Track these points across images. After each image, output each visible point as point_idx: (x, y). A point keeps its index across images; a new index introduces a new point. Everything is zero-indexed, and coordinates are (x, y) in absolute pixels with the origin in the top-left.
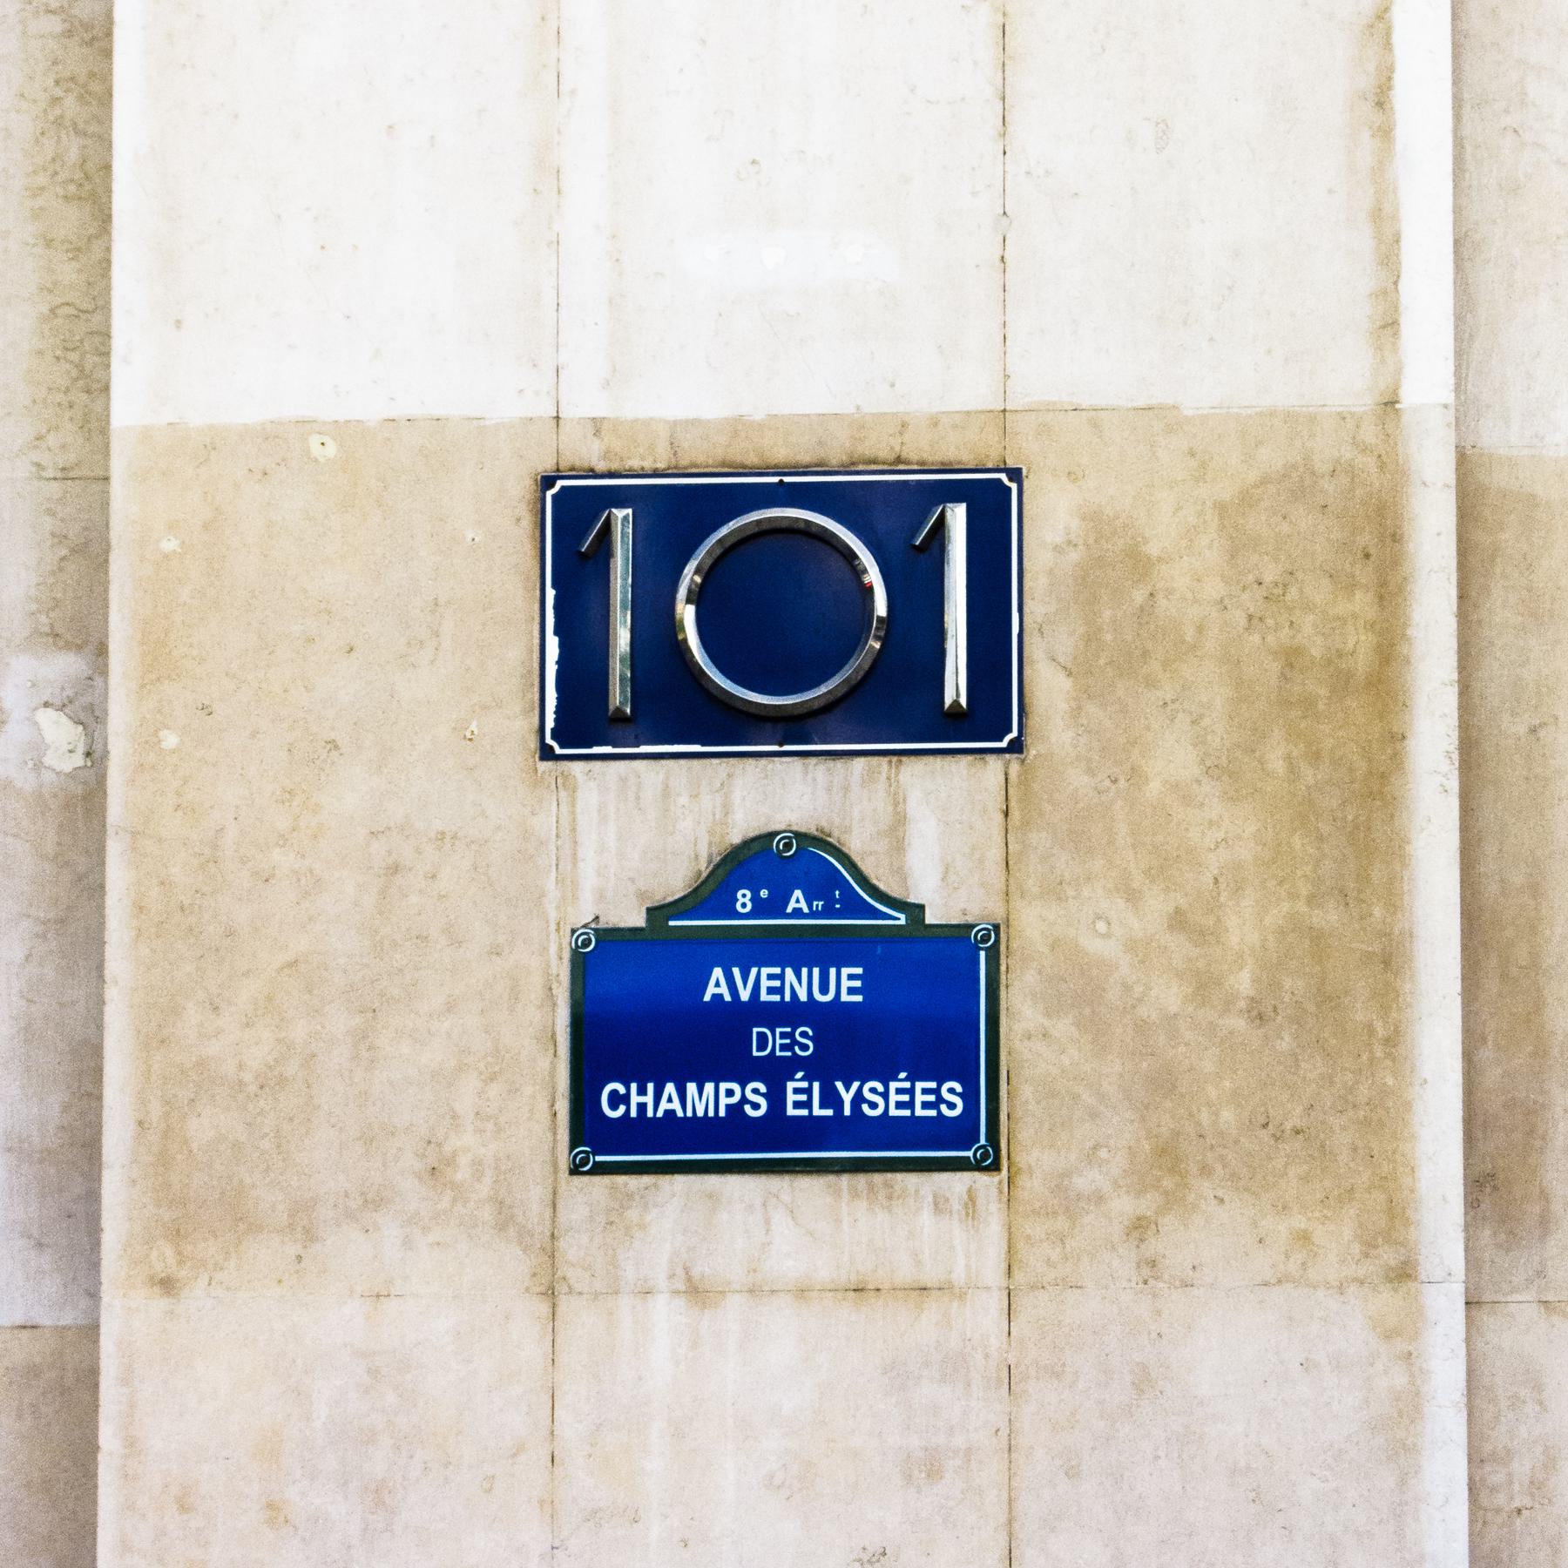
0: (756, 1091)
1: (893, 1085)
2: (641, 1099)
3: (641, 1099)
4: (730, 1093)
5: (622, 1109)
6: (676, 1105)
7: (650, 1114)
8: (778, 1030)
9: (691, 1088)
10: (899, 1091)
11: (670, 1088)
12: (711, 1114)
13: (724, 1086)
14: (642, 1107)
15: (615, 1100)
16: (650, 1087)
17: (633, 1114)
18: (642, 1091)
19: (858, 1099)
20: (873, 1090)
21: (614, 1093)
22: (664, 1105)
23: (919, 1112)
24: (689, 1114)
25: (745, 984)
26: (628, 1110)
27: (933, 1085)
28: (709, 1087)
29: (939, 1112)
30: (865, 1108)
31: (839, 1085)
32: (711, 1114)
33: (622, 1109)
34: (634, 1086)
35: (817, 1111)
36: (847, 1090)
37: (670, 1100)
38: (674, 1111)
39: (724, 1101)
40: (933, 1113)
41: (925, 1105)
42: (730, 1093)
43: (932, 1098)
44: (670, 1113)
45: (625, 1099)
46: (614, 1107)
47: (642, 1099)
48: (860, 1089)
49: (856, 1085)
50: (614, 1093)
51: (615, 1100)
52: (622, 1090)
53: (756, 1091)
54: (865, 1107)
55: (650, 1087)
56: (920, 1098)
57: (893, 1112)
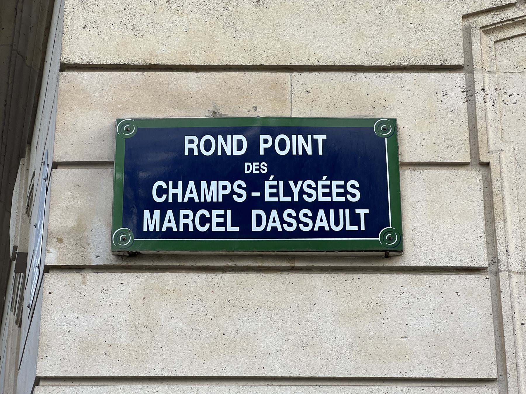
0: (239, 186)
1: (320, 183)
4: (225, 188)
6: (195, 195)
7: (180, 200)
9: (204, 184)
10: (324, 187)
11: (191, 184)
14: (175, 195)
15: (161, 191)
16: (180, 183)
17: (170, 200)
18: (175, 186)
19: (302, 192)
20: (309, 186)
21: (160, 187)
24: (202, 200)
29: (346, 199)
30: (305, 197)
33: (165, 196)
34: (171, 183)
38: (193, 198)
41: (339, 195)
43: (342, 190)
45: (166, 191)
46: (159, 196)
47: (175, 191)
50: (160, 187)
51: (161, 191)
53: (239, 186)
54: (305, 197)
55: (180, 183)
56: (335, 191)
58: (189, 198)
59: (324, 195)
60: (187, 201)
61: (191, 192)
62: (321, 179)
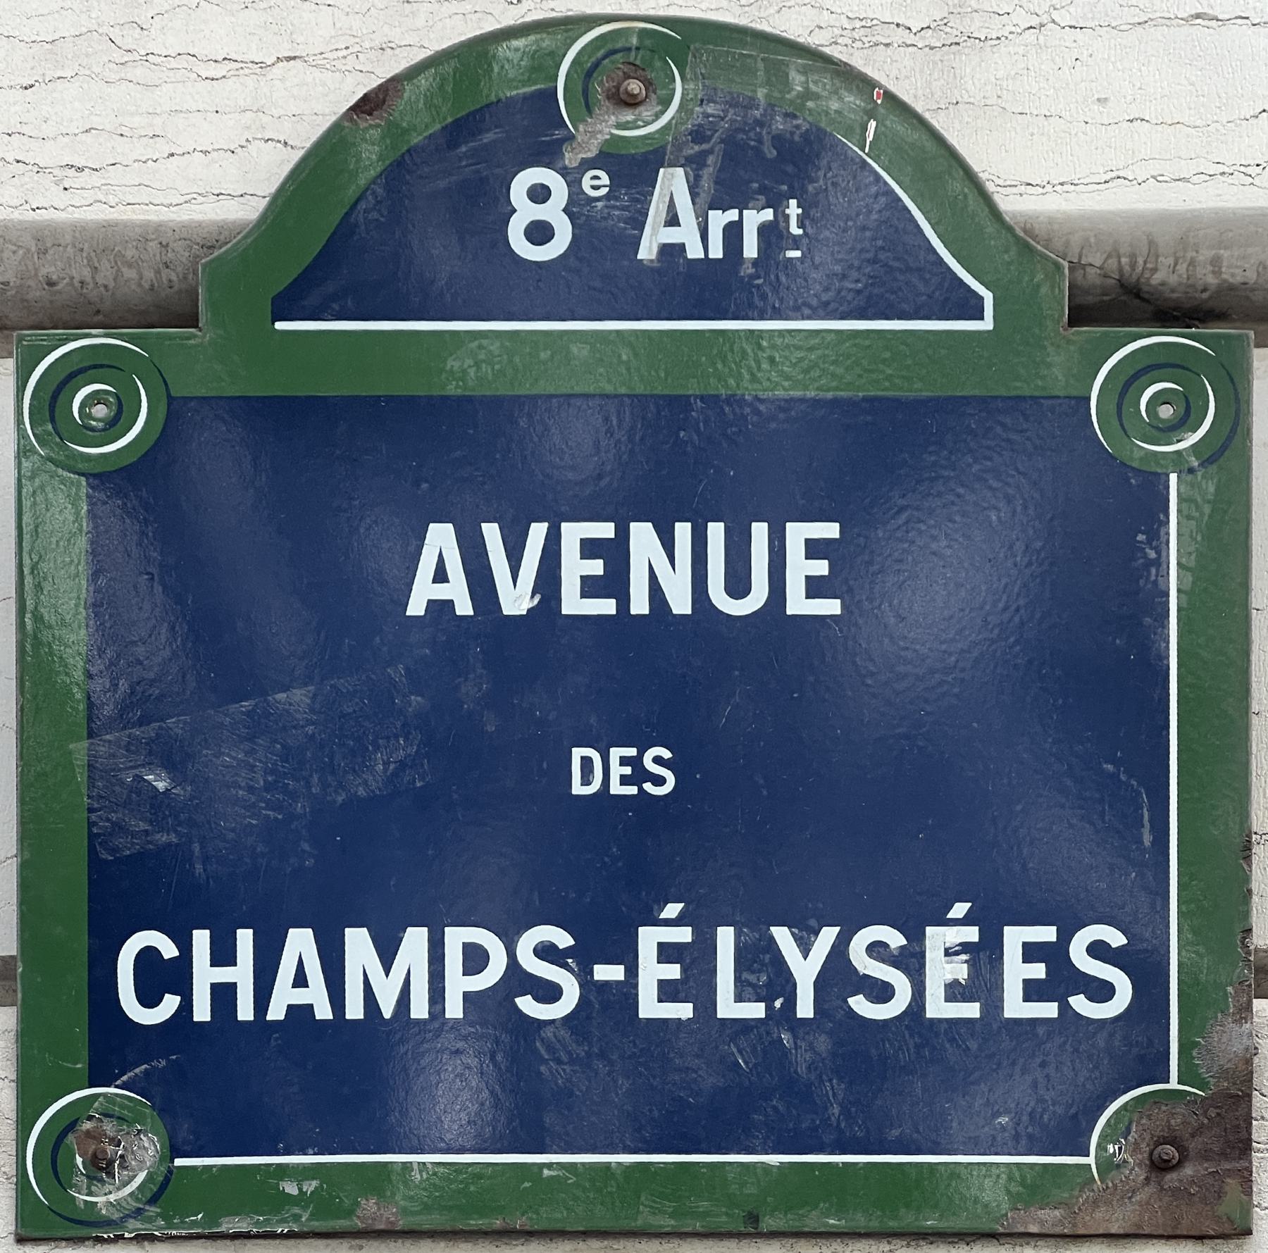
1: (938, 938)
2: (218, 974)
3: (218, 974)
5: (170, 1003)
7: (245, 1011)
9: (358, 945)
11: (300, 943)
12: (420, 1009)
13: (456, 938)
14: (224, 995)
16: (245, 939)
17: (202, 1012)
18: (223, 955)
19: (838, 977)
20: (877, 950)
21: (147, 956)
23: (1015, 1007)
28: (415, 940)
29: (1065, 1008)
31: (782, 936)
32: (420, 1009)
33: (170, 1003)
34: (201, 939)
35: (728, 1007)
39: (458, 985)
40: (1049, 1010)
41: (1032, 991)
42: (475, 959)
44: (300, 1013)
46: (148, 998)
47: (224, 975)
48: (839, 952)
49: (828, 935)
50: (147, 956)
51: (159, 977)
52: (169, 950)
55: (245, 939)
56: (1017, 972)
57: (938, 1008)
58: (291, 1008)
59: (954, 992)
60: (280, 1016)
61: (300, 980)
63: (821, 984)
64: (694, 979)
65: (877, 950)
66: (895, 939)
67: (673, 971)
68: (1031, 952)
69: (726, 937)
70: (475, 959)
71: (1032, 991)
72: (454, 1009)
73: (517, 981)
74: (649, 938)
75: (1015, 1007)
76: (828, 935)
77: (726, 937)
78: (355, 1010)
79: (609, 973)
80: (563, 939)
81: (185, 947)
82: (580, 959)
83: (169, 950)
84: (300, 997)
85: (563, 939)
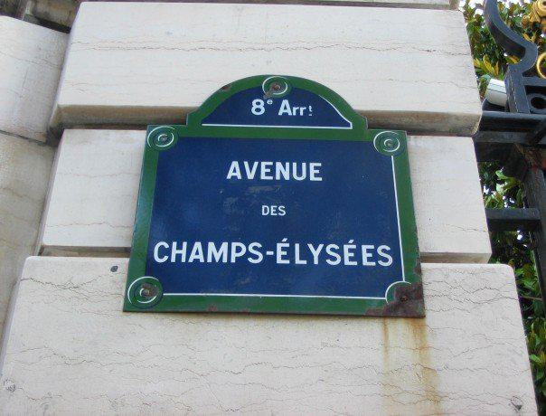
1: (346, 247)
2: (178, 252)
3: (178, 252)
5: (166, 258)
7: (183, 260)
8: (272, 207)
9: (211, 246)
11: (198, 245)
12: (225, 260)
13: (234, 245)
14: (179, 256)
15: (163, 252)
16: (185, 244)
17: (173, 260)
18: (179, 247)
19: (323, 255)
20: (332, 250)
22: (193, 257)
25: (251, 169)
26: (170, 259)
27: (372, 247)
28: (225, 246)
29: (377, 264)
31: (311, 246)
32: (225, 260)
33: (166, 258)
34: (175, 244)
35: (298, 261)
36: (316, 248)
37: (197, 252)
39: (234, 255)
40: (374, 264)
41: (369, 259)
42: (239, 249)
44: (196, 261)
45: (168, 252)
46: (161, 257)
47: (179, 252)
49: (321, 246)
52: (167, 246)
55: (185, 244)
56: (365, 255)
57: (347, 262)
59: (351, 259)
61: (197, 253)
62: (347, 243)
63: (320, 257)
64: (290, 254)
65: (332, 250)
66: (337, 247)
67: (285, 253)
68: (368, 251)
69: (297, 246)
70: (239, 249)
71: (369, 259)
72: (233, 260)
73: (248, 254)
74: (279, 246)
75: (365, 262)
76: (321, 246)
77: (297, 246)
78: (209, 260)
79: (270, 253)
80: (259, 245)
81: (171, 246)
82: (262, 250)
83: (167, 246)
84: (197, 257)
85: (259, 245)
